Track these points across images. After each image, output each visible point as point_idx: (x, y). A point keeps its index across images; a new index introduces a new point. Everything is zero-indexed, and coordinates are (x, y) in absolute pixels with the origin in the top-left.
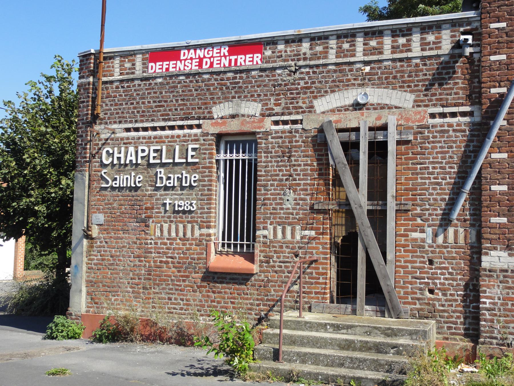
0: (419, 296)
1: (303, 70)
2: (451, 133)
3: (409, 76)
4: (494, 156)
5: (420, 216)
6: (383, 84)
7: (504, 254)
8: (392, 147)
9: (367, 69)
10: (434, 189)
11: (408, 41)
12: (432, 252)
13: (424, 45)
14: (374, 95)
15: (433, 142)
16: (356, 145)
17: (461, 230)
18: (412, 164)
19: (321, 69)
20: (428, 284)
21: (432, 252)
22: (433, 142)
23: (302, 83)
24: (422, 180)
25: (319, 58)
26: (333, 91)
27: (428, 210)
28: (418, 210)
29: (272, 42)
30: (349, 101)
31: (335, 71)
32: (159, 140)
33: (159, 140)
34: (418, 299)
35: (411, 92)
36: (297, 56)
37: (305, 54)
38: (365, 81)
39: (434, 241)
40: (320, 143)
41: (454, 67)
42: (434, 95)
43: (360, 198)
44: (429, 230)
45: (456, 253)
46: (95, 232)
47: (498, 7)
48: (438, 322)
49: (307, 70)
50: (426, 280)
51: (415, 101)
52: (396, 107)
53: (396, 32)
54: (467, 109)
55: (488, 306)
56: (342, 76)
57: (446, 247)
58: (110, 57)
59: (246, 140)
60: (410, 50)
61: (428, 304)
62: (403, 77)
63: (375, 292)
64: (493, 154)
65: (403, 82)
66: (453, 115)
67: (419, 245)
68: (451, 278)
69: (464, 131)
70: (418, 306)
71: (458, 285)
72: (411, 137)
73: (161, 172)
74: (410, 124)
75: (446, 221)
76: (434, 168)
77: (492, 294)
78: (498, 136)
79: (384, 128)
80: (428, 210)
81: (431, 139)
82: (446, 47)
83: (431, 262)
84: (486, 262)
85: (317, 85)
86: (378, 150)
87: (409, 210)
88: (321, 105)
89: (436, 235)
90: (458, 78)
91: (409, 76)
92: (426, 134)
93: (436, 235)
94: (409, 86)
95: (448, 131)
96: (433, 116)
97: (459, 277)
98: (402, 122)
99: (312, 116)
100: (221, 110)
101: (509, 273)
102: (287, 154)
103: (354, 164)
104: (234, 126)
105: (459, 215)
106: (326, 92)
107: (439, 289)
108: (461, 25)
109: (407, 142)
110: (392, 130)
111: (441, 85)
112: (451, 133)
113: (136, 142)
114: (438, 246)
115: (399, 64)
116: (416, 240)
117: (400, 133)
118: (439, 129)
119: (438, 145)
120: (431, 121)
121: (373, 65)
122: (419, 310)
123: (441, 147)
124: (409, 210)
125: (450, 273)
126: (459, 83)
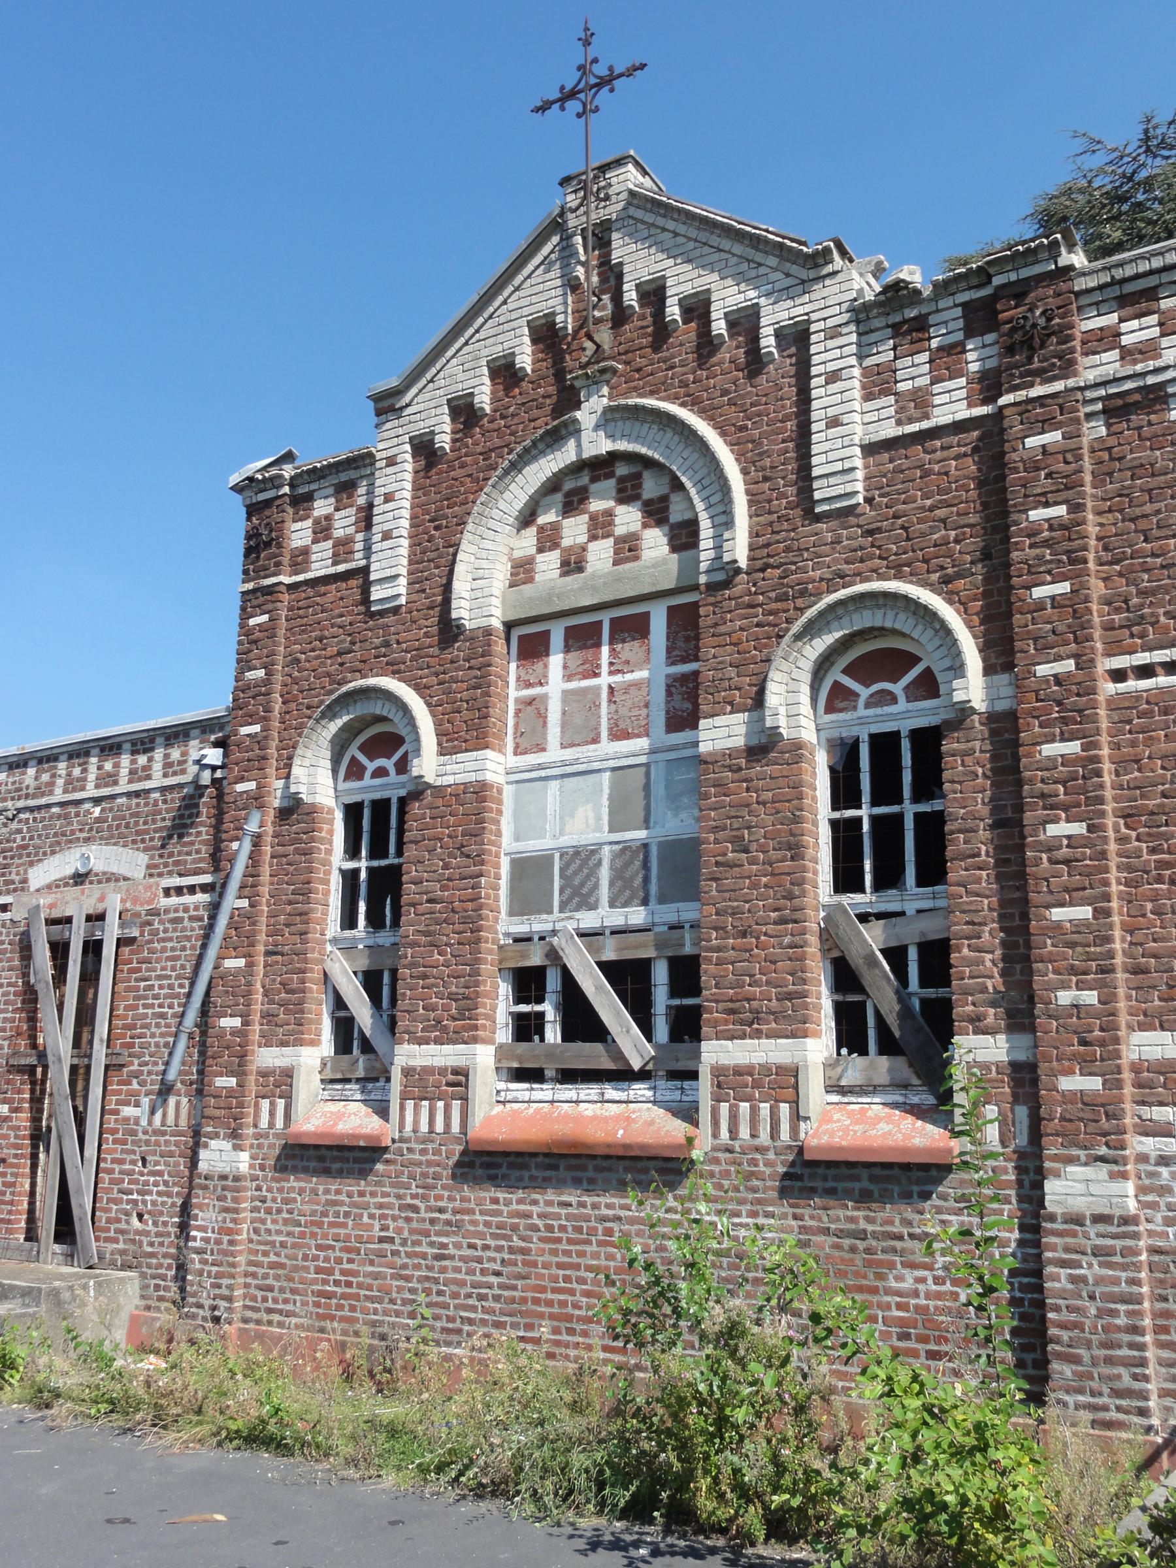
0: (123, 1226)
1: (22, 816)
2: (186, 923)
3: (145, 823)
4: (230, 963)
5: (136, 1075)
6: (112, 837)
7: (226, 1145)
9: (97, 811)
10: (158, 1025)
11: (150, 760)
12: (147, 1143)
14: (100, 857)
15: (164, 940)
16: (66, 945)
17: (185, 1100)
18: (137, 980)
19: (43, 813)
20: (135, 1202)
21: (147, 1143)
22: (164, 940)
23: (19, 837)
24: (151, 1008)
25: (43, 794)
26: (53, 853)
27: (146, 1064)
28: (135, 1067)
30: (69, 871)
31: (59, 817)
34: (122, 1232)
35: (146, 850)
37: (27, 787)
39: (150, 1123)
41: (197, 806)
42: (171, 855)
44: (145, 1101)
45: (177, 1144)
47: (254, 697)
48: (143, 1276)
49: (27, 815)
50: (135, 1196)
51: (148, 867)
52: (126, 879)
54: (207, 879)
55: (198, 1244)
57: (164, 1133)
60: (149, 777)
61: (133, 1241)
62: (136, 823)
65: (138, 833)
66: (192, 890)
69: (201, 919)
70: (121, 1246)
71: (173, 1205)
72: (135, 933)
74: (138, 908)
76: (161, 987)
78: (229, 926)
79: (101, 917)
80: (146, 1064)
81: (162, 935)
83: (144, 1160)
85: (36, 841)
87: (123, 1066)
88: (42, 874)
89: (153, 1112)
90: (202, 824)
91: (145, 823)
92: (156, 925)
93: (153, 1112)
94: (143, 841)
95: (182, 919)
96: (167, 892)
97: (176, 1189)
98: (128, 905)
99: (25, 898)
101: (229, 1183)
105: (180, 1073)
106: (45, 854)
107: (149, 1213)
108: (212, 732)
109: (133, 940)
110: (112, 921)
111: (181, 836)
112: (186, 923)
114: (156, 1132)
115: (135, 801)
116: (126, 1120)
117: (122, 926)
118: (172, 915)
119: (169, 945)
120: (164, 902)
121: (104, 805)
122: (123, 1252)
123: (173, 949)
124: (123, 1066)
125: (166, 1183)
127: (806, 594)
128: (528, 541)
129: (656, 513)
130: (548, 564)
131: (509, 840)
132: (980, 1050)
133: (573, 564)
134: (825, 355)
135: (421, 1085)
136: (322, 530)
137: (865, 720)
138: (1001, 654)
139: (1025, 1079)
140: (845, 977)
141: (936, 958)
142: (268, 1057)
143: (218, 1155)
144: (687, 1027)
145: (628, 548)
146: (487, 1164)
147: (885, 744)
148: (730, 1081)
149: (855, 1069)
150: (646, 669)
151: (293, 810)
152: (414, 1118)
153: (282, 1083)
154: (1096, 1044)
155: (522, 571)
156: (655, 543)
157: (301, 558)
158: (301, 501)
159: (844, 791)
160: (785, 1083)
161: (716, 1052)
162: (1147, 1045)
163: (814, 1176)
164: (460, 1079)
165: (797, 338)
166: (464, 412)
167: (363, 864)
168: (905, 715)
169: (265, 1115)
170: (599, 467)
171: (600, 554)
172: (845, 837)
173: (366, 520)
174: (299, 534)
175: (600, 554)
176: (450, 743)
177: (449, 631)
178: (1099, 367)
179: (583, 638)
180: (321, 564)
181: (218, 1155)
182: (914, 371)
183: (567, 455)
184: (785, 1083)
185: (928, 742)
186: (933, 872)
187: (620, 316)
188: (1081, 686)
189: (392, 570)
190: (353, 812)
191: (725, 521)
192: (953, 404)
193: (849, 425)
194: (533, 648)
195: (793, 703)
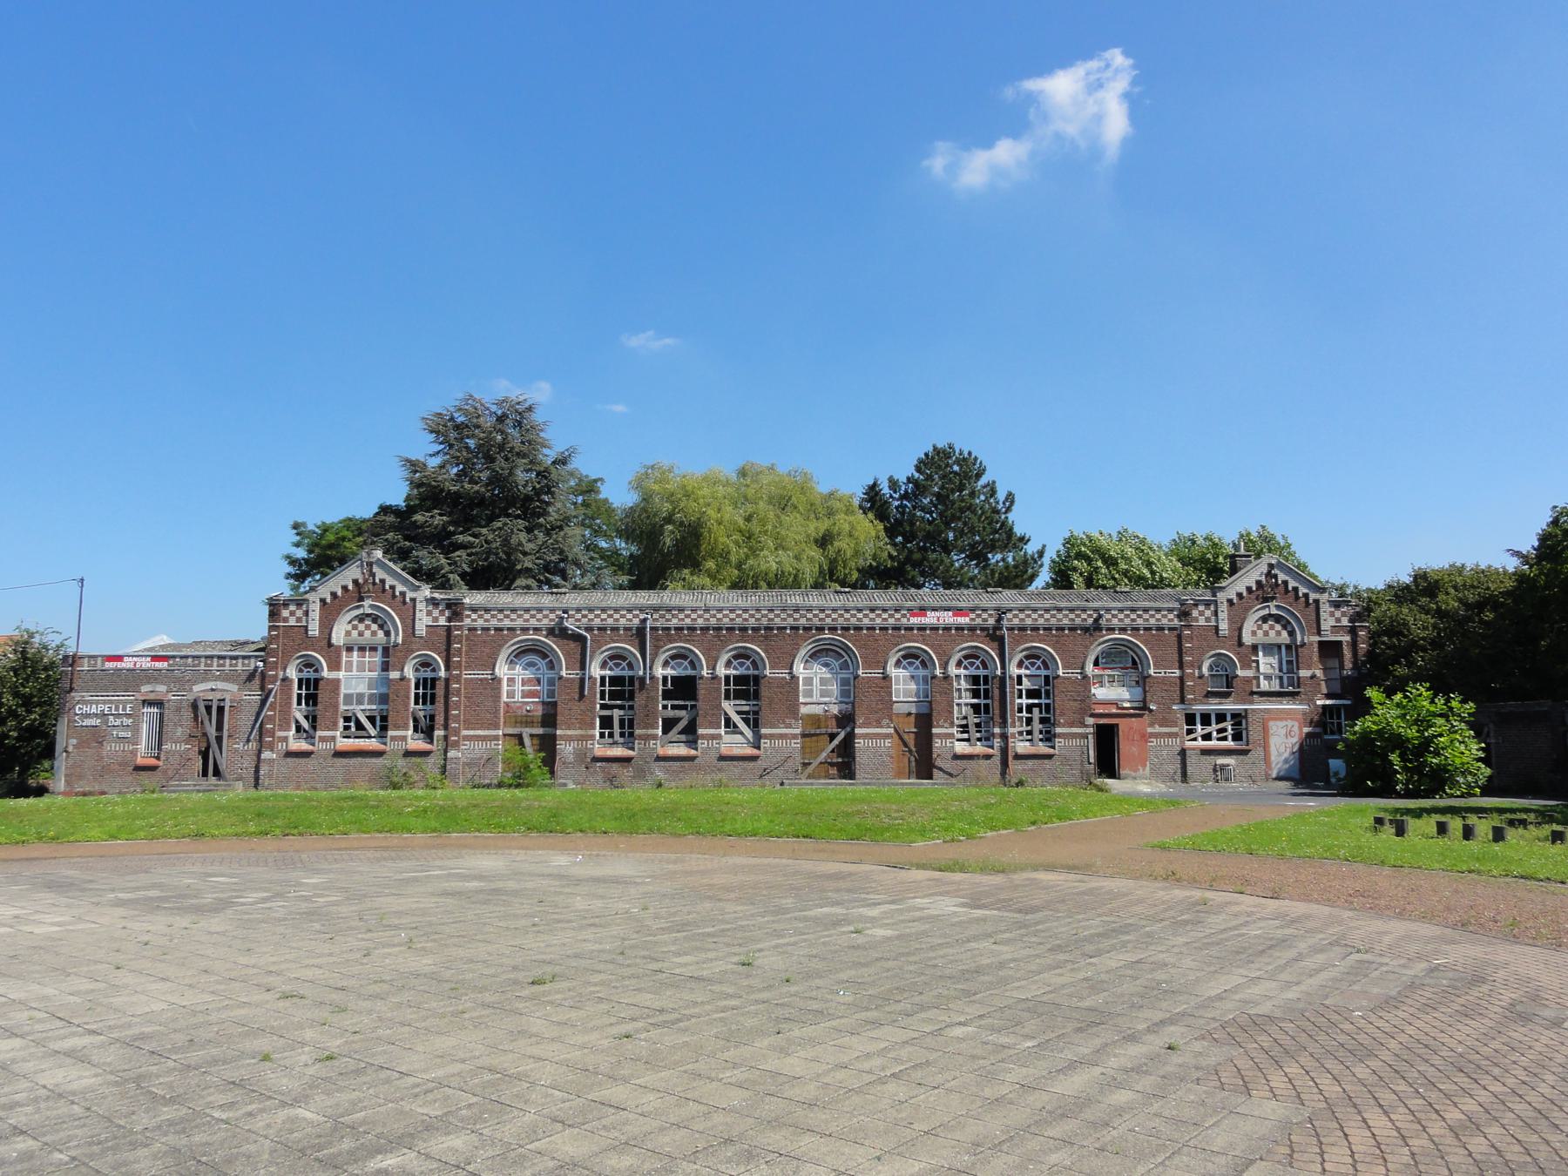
8: (227, 709)
14: (220, 685)
29: (174, 657)
32: (111, 702)
33: (111, 702)
36: (186, 665)
38: (217, 679)
40: (194, 706)
43: (212, 731)
46: (70, 749)
53: (233, 658)
56: (206, 676)
58: (82, 657)
59: (159, 704)
63: (217, 773)
64: (267, 712)
67: (236, 750)
68: (249, 763)
75: (248, 741)
86: (221, 710)
88: (196, 688)
100: (145, 689)
102: (179, 709)
103: (209, 713)
104: (152, 697)
113: (97, 703)
126: (257, 681)
127: (413, 651)
129: (381, 627)
130: (355, 633)
131: (343, 690)
132: (439, 733)
133: (361, 634)
135: (322, 739)
136: (292, 613)
137: (422, 675)
138: (448, 668)
139: (446, 738)
140: (415, 720)
141: (432, 718)
143: (266, 755)
144: (384, 728)
145: (374, 633)
146: (339, 754)
147: (425, 680)
148: (393, 738)
149: (416, 736)
150: (378, 658)
151: (285, 679)
152: (321, 746)
153: (285, 739)
155: (348, 633)
156: (381, 634)
157: (285, 620)
158: (286, 604)
159: (417, 687)
160: (404, 738)
161: (390, 733)
162: (465, 733)
163: (408, 754)
164: (333, 738)
165: (414, 600)
166: (334, 595)
167: (304, 692)
168: (429, 675)
169: (281, 746)
170: (368, 615)
171: (367, 634)
172: (417, 695)
173: (307, 613)
174: (285, 613)
175: (367, 634)
176: (330, 669)
177: (330, 645)
178: (467, 621)
179: (362, 649)
180: (292, 622)
182: (436, 613)
183: (361, 611)
184: (404, 738)
185: (434, 680)
186: (433, 703)
187: (374, 583)
188: (459, 676)
189: (314, 629)
190: (300, 681)
191: (397, 634)
192: (442, 621)
193: (423, 622)
194: (349, 649)
195: (409, 671)
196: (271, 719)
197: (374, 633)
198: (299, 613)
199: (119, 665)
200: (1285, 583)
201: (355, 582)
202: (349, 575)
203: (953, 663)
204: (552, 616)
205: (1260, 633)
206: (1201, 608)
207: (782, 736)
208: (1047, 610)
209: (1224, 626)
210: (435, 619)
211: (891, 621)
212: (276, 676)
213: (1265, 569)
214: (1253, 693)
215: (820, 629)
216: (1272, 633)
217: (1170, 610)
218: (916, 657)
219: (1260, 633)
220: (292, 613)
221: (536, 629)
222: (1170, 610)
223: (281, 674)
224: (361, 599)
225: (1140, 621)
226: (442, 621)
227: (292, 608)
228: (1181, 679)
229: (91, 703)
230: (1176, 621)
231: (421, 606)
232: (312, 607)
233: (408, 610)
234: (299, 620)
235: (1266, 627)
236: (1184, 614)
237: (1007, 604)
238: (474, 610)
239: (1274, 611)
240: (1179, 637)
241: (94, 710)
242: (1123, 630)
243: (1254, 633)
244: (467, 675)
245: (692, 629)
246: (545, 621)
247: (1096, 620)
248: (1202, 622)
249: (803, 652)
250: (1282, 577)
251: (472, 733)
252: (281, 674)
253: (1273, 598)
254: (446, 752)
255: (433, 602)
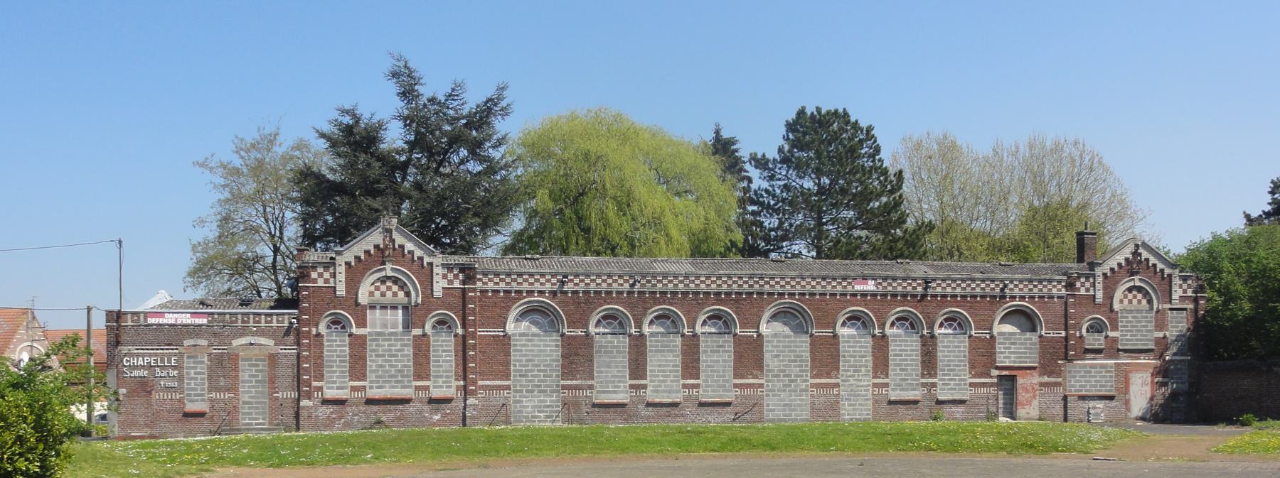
13: (278, 321)
32: (156, 355)
33: (156, 355)
36: (223, 321)
56: (244, 332)
58: (126, 313)
73: (158, 370)
77: (304, 414)
82: (286, 324)
84: (302, 404)
113: (143, 356)
128: (372, 288)
129: (401, 288)
130: (377, 294)
133: (383, 295)
134: (436, 270)
138: (464, 326)
142: (315, 384)
145: (395, 294)
154: (474, 382)
155: (371, 294)
156: (401, 294)
157: (315, 281)
158: (314, 268)
162: (480, 383)
165: (431, 264)
170: (389, 278)
171: (389, 294)
173: (334, 275)
174: (314, 275)
175: (389, 294)
177: (357, 304)
178: (479, 284)
180: (321, 283)
181: (305, 403)
182: (450, 276)
183: (383, 274)
187: (394, 249)
188: (475, 333)
189: (341, 290)
191: (417, 296)
192: (457, 284)
196: (307, 371)
197: (395, 294)
198: (326, 275)
199: (161, 321)
200: (1147, 260)
201: (377, 247)
202: (372, 239)
203: (888, 324)
204: (554, 281)
205: (1126, 301)
206: (1083, 280)
207: (749, 386)
208: (963, 280)
209: (1099, 295)
210: (451, 282)
211: (839, 288)
212: (309, 332)
213: (1131, 248)
214: (1119, 350)
215: (781, 295)
216: (1135, 302)
217: (1059, 282)
218: (858, 319)
219: (1126, 301)
220: (321, 275)
221: (541, 293)
222: (1059, 282)
223: (314, 331)
224: (383, 263)
225: (1035, 290)
226: (457, 284)
227: (320, 270)
228: (1066, 339)
229: (138, 355)
230: (1064, 292)
231: (438, 270)
232: (338, 269)
233: (426, 275)
234: (326, 281)
235: (1130, 296)
236: (1070, 286)
237: (931, 273)
238: (485, 275)
239: (1138, 284)
240: (1066, 303)
241: (141, 362)
242: (1022, 298)
243: (1121, 301)
244: (482, 332)
245: (674, 294)
246: (548, 285)
247: (1002, 290)
248: (1083, 292)
249: (767, 315)
250: (1145, 254)
251: (488, 383)
252: (314, 331)
253: (1137, 273)
254: (299, 400)
255: (449, 268)
